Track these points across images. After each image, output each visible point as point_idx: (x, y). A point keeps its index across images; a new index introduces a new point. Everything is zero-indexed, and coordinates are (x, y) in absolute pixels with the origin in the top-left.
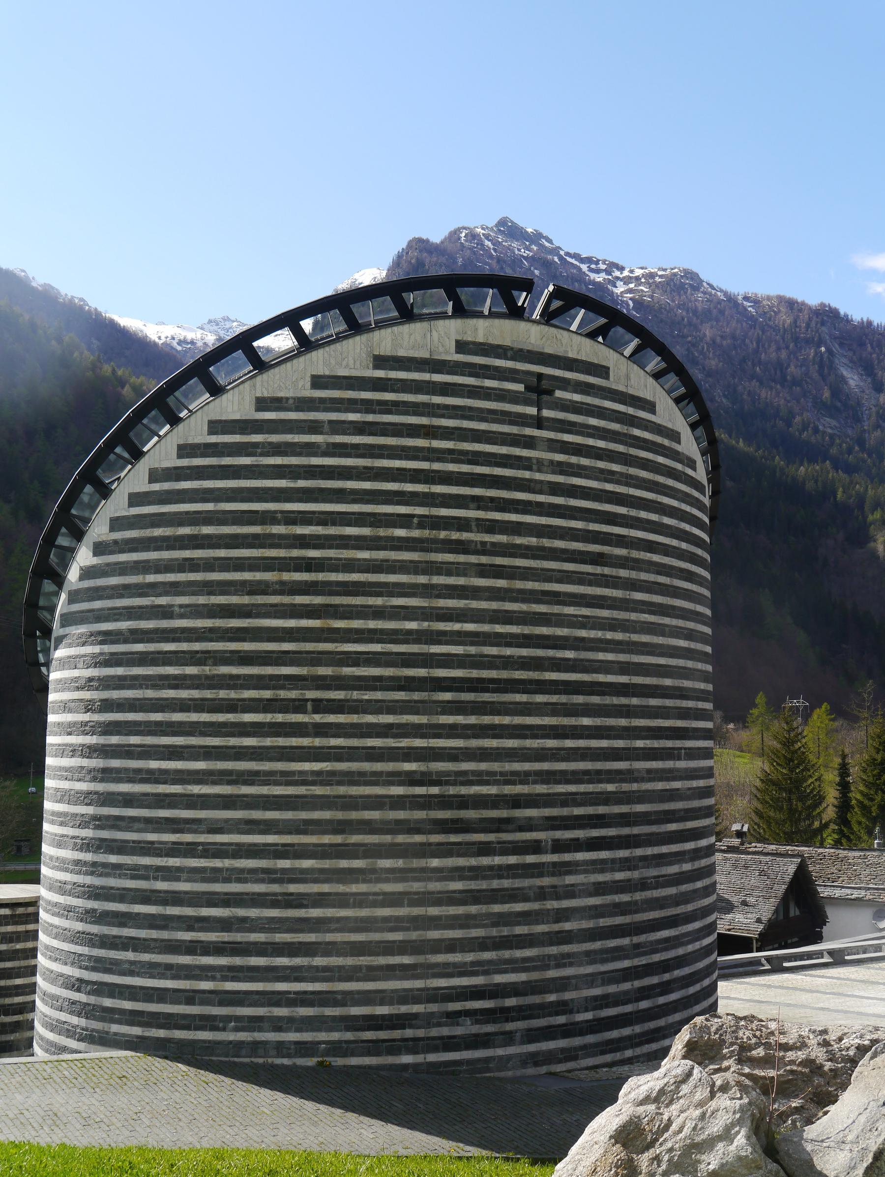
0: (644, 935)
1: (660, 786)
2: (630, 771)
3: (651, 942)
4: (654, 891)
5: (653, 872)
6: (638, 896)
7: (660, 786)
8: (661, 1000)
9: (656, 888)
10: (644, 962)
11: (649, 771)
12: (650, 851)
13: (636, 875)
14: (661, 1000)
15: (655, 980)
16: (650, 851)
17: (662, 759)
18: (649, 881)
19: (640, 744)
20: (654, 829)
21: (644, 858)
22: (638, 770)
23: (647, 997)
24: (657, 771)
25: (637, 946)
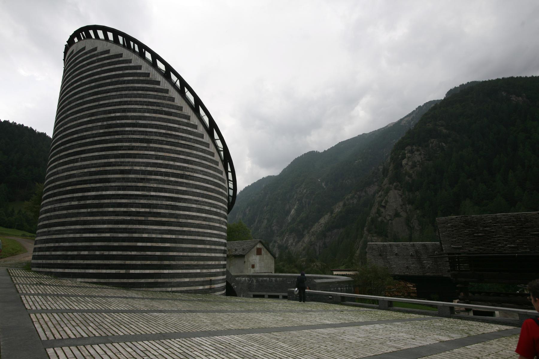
0: (52, 228)
1: (66, 174)
2: (57, 171)
3: (53, 230)
4: (57, 212)
5: (58, 205)
6: (52, 214)
7: (66, 174)
8: (53, 253)
9: (58, 211)
10: (50, 238)
11: (62, 169)
12: (58, 198)
13: (53, 206)
14: (53, 253)
15: (52, 245)
16: (58, 198)
17: (68, 164)
18: (56, 208)
19: (61, 161)
20: (61, 190)
21: (56, 200)
22: (59, 170)
23: (49, 251)
24: (65, 169)
25: (49, 231)
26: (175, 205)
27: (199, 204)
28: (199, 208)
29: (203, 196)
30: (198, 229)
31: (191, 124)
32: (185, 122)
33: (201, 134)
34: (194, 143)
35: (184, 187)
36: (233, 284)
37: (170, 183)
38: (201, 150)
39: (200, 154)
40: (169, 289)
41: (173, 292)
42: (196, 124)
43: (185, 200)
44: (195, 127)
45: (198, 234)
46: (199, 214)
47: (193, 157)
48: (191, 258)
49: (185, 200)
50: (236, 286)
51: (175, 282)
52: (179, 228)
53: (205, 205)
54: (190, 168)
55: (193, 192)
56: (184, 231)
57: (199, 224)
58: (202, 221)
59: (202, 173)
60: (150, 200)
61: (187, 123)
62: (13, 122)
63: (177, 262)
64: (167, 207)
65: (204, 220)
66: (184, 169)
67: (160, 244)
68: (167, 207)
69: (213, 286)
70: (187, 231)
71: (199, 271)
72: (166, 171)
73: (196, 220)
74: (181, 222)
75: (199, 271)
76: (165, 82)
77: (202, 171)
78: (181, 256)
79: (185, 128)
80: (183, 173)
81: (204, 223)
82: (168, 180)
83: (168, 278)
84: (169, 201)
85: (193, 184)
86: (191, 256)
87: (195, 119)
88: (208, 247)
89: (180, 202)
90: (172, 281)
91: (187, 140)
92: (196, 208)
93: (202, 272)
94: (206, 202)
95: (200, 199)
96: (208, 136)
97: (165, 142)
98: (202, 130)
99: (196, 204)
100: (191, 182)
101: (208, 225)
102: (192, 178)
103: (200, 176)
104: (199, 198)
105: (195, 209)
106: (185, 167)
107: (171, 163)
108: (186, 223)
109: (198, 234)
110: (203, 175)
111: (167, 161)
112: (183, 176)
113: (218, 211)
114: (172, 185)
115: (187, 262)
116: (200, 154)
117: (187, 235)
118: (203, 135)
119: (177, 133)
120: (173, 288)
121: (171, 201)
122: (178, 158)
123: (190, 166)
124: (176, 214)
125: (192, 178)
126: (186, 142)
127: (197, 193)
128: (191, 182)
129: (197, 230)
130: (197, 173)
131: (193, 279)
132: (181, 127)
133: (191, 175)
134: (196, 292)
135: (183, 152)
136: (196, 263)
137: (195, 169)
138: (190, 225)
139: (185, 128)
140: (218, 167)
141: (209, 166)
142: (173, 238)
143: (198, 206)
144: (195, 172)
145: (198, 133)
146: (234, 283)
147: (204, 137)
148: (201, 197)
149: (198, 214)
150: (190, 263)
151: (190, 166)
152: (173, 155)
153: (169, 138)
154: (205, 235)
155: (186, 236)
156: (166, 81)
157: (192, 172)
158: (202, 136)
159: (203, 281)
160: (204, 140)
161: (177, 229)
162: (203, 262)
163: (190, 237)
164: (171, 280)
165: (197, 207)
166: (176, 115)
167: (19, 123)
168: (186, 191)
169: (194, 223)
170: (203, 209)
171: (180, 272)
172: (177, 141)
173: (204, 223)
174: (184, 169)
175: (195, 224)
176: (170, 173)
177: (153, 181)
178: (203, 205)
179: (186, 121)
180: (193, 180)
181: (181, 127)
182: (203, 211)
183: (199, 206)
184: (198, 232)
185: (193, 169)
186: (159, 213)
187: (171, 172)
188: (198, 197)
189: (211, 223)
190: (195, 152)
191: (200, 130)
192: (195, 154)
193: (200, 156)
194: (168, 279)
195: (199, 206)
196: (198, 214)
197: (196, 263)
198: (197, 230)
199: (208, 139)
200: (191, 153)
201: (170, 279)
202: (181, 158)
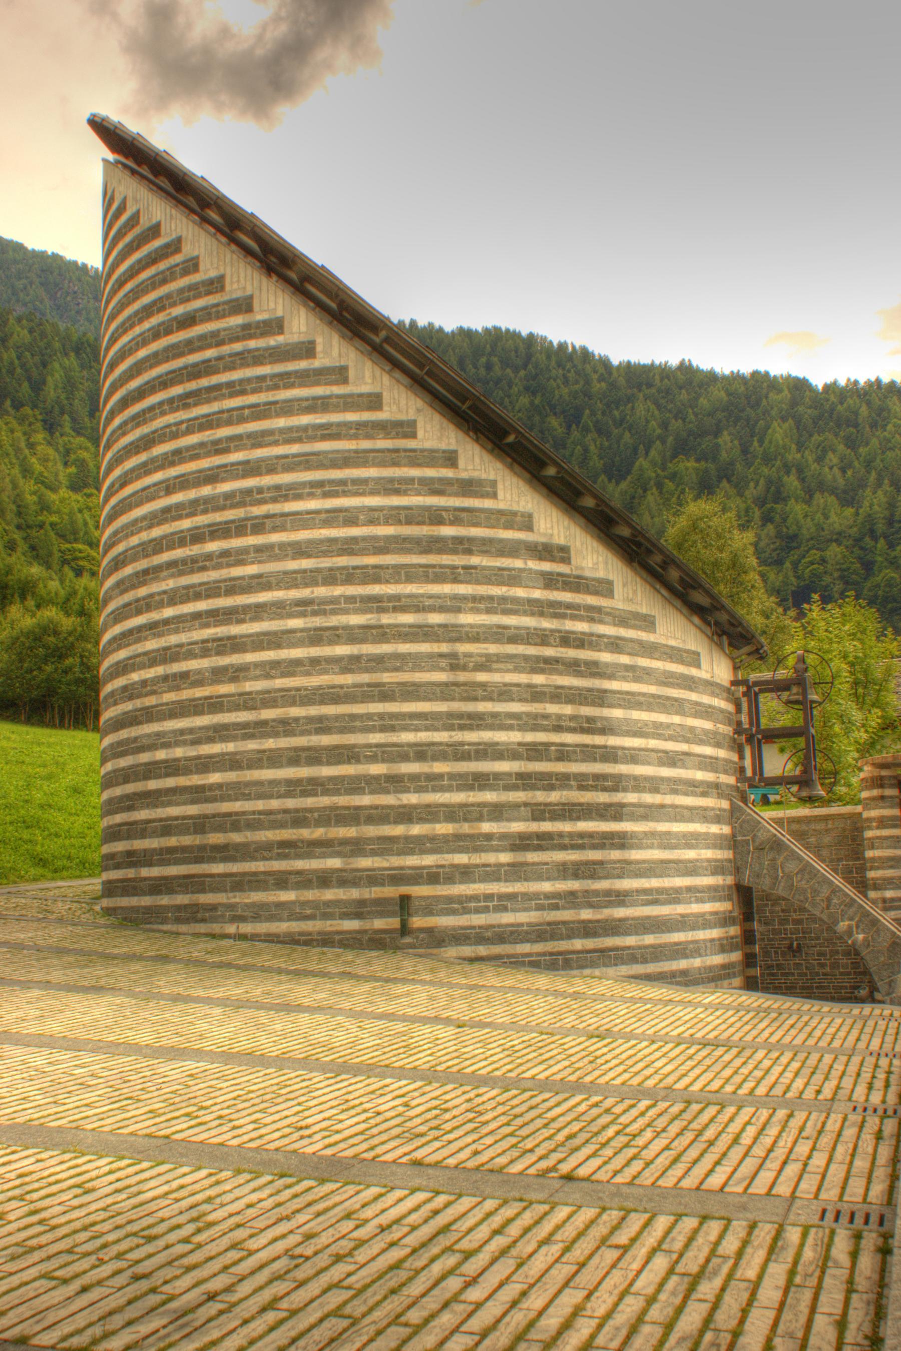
26: (228, 634)
27: (315, 613)
28: (316, 629)
29: (331, 577)
30: (317, 707)
31: (258, 322)
32: (237, 326)
33: (303, 343)
34: (276, 387)
35: (253, 563)
36: (847, 923)
37: (208, 563)
38: (305, 404)
39: (306, 420)
40: (231, 929)
41: (243, 937)
42: (280, 313)
43: (258, 612)
44: (276, 326)
45: (321, 725)
46: (318, 649)
47: (276, 443)
48: (299, 819)
49: (258, 612)
50: (861, 937)
51: (246, 905)
52: (245, 713)
53: (346, 612)
54: (269, 489)
55: (285, 573)
56: (264, 723)
57: (320, 688)
58: (335, 673)
59: (319, 491)
60: (163, 635)
61: (246, 327)
62: (849, 380)
63: (249, 834)
64: (206, 649)
65: (346, 670)
66: (246, 497)
67: (196, 777)
68: (206, 649)
69: (417, 922)
70: (274, 720)
71: (335, 863)
72: (194, 525)
73: (308, 674)
74: (250, 693)
75: (335, 863)
76: (171, 216)
77: (321, 484)
78: (260, 813)
79: (238, 347)
80: (242, 515)
81: (348, 679)
82: (201, 555)
83: (226, 891)
84: (207, 625)
85: (282, 546)
86: (297, 811)
87: (272, 298)
88: (377, 769)
89: (241, 621)
90: (237, 900)
91: (248, 388)
92: (302, 630)
93: (354, 866)
94: (351, 599)
95: (321, 591)
96: (336, 339)
97: (184, 426)
98: (303, 329)
99: (303, 615)
100: (276, 538)
101: (369, 685)
102: (278, 521)
103: (313, 504)
104: (315, 589)
105: (299, 635)
106: (248, 492)
107: (206, 491)
108: (268, 692)
109: (321, 725)
110: (326, 495)
111: (194, 491)
112: (246, 526)
113: (435, 618)
114: (215, 568)
115: (284, 831)
116: (306, 420)
117: (276, 735)
118: (312, 343)
119: (215, 380)
120: (241, 925)
121: (215, 626)
122: (225, 466)
123: (267, 480)
124: (232, 665)
125: (278, 521)
126: (245, 398)
127: (305, 571)
128: (276, 538)
129: (314, 711)
130: (298, 497)
131: (310, 895)
132: (226, 349)
133: (271, 512)
134: (326, 940)
135: (238, 437)
136: (319, 833)
137: (287, 485)
138: (283, 696)
139: (238, 347)
140: (411, 444)
141: (356, 451)
142: (227, 754)
143: (314, 619)
144: (286, 498)
145: (287, 344)
146: (851, 919)
147: (319, 348)
148: (324, 584)
149: (315, 652)
150: (294, 837)
151: (267, 480)
152: (209, 460)
153: (196, 405)
154: (354, 727)
155: (271, 740)
156: (174, 212)
157: (274, 500)
158: (308, 350)
159: (362, 903)
160: (317, 363)
161: (239, 720)
162: (354, 829)
163: (289, 739)
164: (235, 897)
165: (309, 625)
166: (208, 314)
167: (829, 380)
168: (260, 576)
169: (298, 689)
170: (335, 628)
171: (262, 869)
172: (215, 407)
173: (348, 679)
174: (248, 499)
175: (306, 689)
176: (205, 526)
177: (167, 568)
178: (334, 612)
179: (237, 320)
180: (282, 528)
181: (226, 349)
182: (338, 636)
183: (318, 621)
184: (320, 719)
185: (278, 488)
186: (185, 675)
187: (206, 522)
188: (307, 585)
189: (386, 675)
190: (281, 422)
191: (295, 329)
192: (282, 431)
193: (305, 428)
194: (224, 894)
195: (318, 621)
196: (315, 652)
197: (319, 833)
198: (314, 711)
199: (335, 352)
200: (265, 433)
201: (231, 895)
202: (233, 464)
